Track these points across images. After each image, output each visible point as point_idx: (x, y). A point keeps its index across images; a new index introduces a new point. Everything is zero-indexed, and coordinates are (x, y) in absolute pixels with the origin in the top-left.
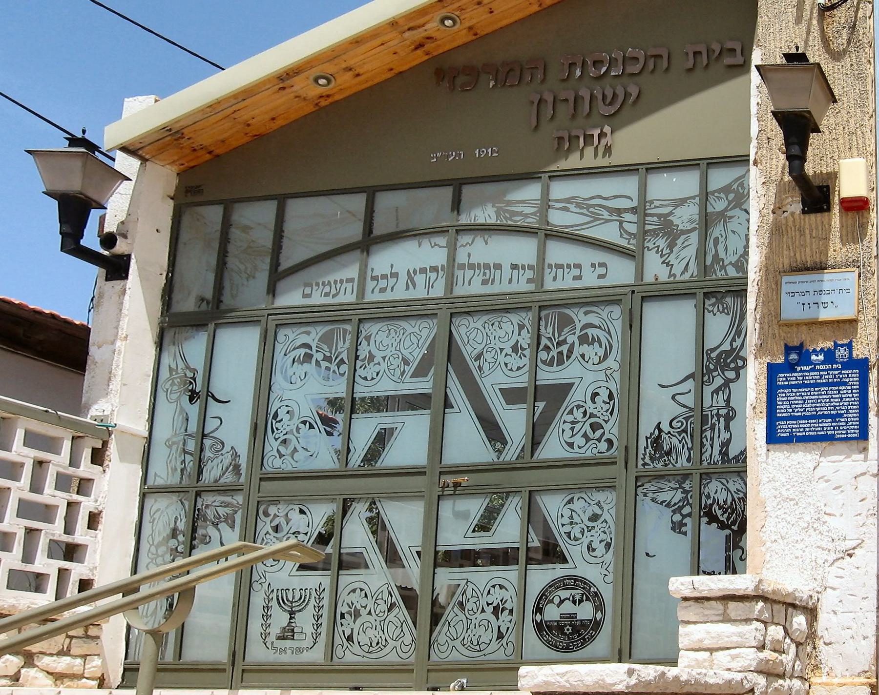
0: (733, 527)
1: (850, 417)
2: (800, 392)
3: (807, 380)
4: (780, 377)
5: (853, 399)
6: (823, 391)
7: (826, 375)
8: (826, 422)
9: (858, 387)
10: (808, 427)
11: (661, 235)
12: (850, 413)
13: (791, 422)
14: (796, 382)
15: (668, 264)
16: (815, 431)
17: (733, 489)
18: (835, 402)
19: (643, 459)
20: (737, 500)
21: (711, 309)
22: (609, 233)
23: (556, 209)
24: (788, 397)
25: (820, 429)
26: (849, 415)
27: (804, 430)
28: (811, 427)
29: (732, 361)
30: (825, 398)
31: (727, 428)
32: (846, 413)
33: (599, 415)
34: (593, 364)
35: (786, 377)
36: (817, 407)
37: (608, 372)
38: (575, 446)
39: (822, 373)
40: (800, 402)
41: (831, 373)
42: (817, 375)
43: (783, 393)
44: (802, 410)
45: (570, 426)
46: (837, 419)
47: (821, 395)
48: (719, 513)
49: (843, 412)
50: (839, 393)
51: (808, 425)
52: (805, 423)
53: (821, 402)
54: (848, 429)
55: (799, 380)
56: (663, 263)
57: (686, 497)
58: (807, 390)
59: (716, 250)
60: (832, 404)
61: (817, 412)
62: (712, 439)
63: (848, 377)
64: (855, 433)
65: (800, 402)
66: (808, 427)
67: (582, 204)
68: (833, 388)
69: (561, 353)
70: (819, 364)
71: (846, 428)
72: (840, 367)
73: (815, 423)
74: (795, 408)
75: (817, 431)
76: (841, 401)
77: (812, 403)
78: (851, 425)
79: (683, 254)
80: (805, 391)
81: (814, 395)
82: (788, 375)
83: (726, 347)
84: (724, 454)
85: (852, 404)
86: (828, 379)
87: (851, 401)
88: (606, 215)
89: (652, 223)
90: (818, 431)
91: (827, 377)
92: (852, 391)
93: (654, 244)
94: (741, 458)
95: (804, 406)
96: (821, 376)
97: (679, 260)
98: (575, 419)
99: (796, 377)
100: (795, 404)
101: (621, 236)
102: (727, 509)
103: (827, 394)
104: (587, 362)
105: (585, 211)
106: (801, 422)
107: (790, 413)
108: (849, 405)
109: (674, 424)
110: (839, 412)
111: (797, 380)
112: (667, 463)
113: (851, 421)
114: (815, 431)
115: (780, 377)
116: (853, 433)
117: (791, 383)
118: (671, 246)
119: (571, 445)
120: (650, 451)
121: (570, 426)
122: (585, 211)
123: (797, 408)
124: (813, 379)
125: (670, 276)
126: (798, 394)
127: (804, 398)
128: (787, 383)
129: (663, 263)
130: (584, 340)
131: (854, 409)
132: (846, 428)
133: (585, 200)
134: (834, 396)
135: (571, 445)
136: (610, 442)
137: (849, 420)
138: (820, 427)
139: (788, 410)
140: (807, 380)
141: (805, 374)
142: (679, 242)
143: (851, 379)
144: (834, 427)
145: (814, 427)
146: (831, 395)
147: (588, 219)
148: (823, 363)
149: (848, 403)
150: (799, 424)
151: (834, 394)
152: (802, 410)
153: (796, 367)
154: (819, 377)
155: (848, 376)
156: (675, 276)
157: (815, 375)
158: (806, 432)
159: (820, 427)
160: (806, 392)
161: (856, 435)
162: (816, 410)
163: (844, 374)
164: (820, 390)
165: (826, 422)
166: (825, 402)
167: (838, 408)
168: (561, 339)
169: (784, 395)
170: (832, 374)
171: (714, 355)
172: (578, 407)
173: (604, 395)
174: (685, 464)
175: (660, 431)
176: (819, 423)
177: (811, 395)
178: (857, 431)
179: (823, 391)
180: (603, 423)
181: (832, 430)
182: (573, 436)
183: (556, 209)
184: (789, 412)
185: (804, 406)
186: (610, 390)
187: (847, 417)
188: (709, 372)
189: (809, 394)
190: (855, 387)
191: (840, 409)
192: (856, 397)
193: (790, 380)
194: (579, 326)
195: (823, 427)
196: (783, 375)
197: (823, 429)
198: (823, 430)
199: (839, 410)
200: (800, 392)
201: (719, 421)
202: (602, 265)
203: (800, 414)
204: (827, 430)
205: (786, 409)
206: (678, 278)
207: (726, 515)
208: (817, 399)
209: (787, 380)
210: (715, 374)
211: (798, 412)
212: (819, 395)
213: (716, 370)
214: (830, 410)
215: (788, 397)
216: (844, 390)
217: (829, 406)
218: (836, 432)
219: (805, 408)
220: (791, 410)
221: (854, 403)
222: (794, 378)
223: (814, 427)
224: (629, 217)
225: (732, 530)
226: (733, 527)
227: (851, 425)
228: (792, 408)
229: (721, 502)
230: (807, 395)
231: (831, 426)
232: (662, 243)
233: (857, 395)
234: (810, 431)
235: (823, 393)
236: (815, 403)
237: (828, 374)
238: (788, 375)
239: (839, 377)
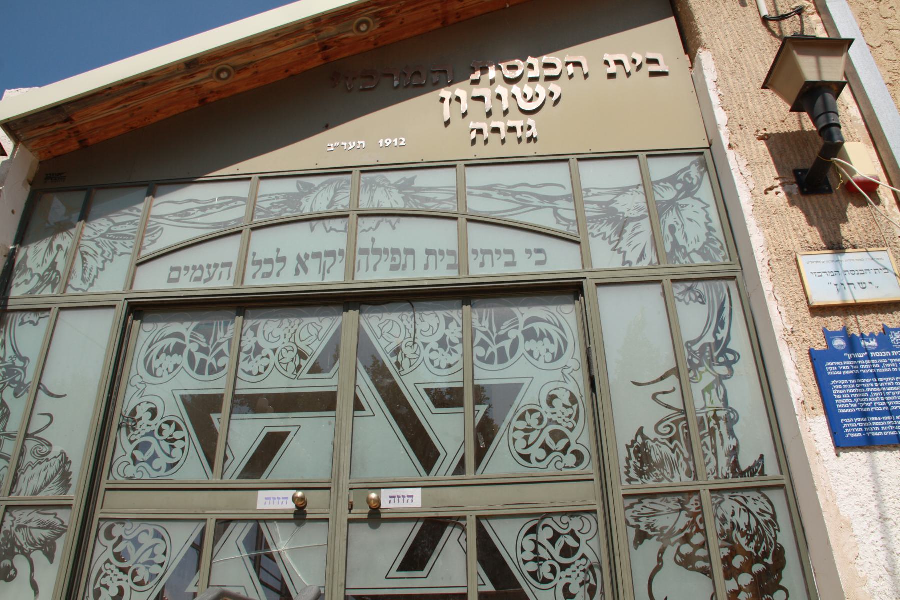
0: (765, 560)
6: (889, 382)
11: (605, 221)
15: (620, 252)
17: (755, 509)
19: (627, 473)
20: (763, 523)
21: (681, 297)
22: (544, 219)
23: (476, 195)
29: (720, 355)
31: (731, 433)
33: (560, 421)
34: (546, 362)
37: (566, 372)
38: (533, 459)
39: (881, 361)
45: (523, 434)
47: (888, 386)
48: (743, 541)
51: (883, 423)
52: (879, 421)
56: (614, 250)
57: (694, 522)
58: (869, 381)
59: (675, 238)
62: (714, 447)
67: (508, 192)
69: (502, 351)
70: (874, 351)
79: (636, 240)
80: (866, 383)
83: (709, 339)
84: (735, 465)
88: (536, 202)
89: (591, 211)
91: (889, 365)
93: (599, 230)
94: (757, 471)
95: (871, 399)
96: (881, 365)
97: (632, 247)
98: (528, 426)
101: (558, 223)
102: (752, 537)
104: (538, 360)
105: (511, 198)
107: (855, 408)
109: (661, 428)
112: (661, 477)
118: (621, 233)
119: (527, 458)
120: (635, 462)
121: (523, 434)
122: (511, 198)
125: (624, 263)
129: (614, 250)
130: (530, 335)
133: (510, 187)
135: (527, 458)
136: (578, 455)
139: (852, 405)
142: (629, 228)
147: (518, 206)
148: (878, 350)
156: (630, 263)
160: (868, 383)
164: (885, 381)
168: (502, 333)
171: (696, 348)
172: (532, 412)
173: (565, 398)
174: (686, 479)
175: (645, 438)
179: (889, 382)
180: (567, 432)
182: (528, 447)
183: (476, 195)
184: (853, 408)
185: (871, 399)
186: (570, 392)
188: (693, 367)
194: (522, 321)
201: (718, 424)
202: (539, 251)
205: (848, 403)
206: (634, 265)
207: (753, 545)
210: (701, 369)
213: (701, 365)
219: (873, 402)
220: (855, 406)
224: (561, 204)
225: (766, 564)
226: (765, 560)
228: (855, 403)
229: (742, 527)
230: (870, 387)
232: (608, 230)
235: (890, 384)
237: (889, 362)
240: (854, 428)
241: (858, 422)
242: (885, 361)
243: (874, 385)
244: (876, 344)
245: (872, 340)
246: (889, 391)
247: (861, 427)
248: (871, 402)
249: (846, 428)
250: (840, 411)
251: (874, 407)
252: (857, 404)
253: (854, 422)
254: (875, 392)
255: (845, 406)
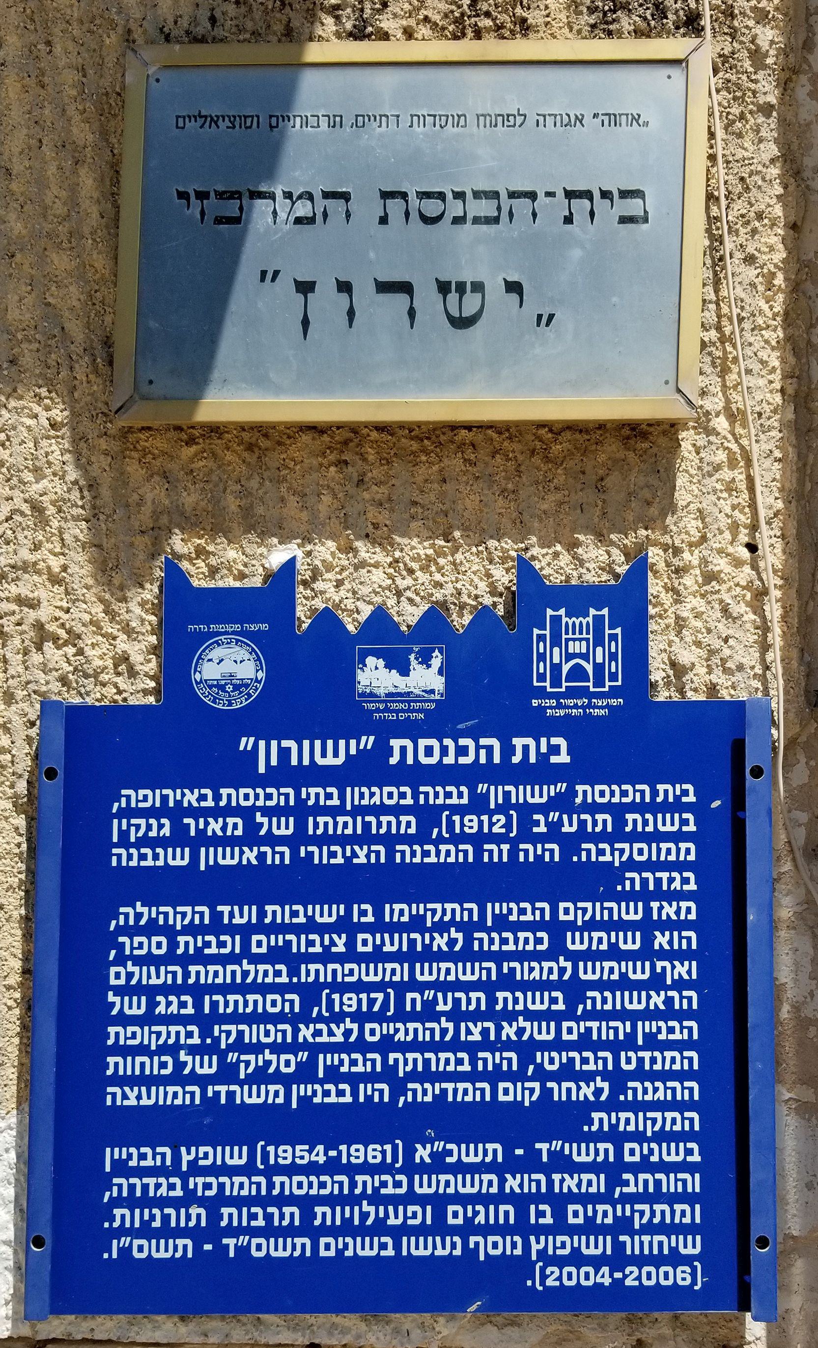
1: (639, 1137)
2: (276, 928)
3: (324, 840)
4: (129, 813)
5: (658, 1000)
6: (441, 927)
7: (461, 810)
8: (460, 1168)
9: (689, 910)
10: (331, 1201)
12: (637, 1106)
13: (208, 1156)
14: (250, 855)
16: (380, 1228)
18: (529, 1015)
24: (185, 961)
25: (417, 1215)
26: (626, 1120)
27: (308, 1215)
28: (353, 1200)
30: (458, 986)
32: (612, 1105)
35: (177, 813)
36: (404, 1047)
40: (273, 1003)
41: (495, 795)
42: (397, 811)
43: (151, 929)
44: (287, 1063)
46: (543, 1147)
47: (430, 956)
49: (587, 1091)
50: (557, 950)
51: (331, 1184)
52: (312, 1169)
53: (429, 1013)
54: (623, 1225)
55: (272, 840)
58: (327, 915)
60: (509, 1031)
61: (398, 1089)
63: (618, 835)
64: (675, 1259)
65: (273, 1003)
66: (331, 1201)
68: (513, 910)
70: (413, 731)
71: (605, 1214)
72: (563, 758)
73: (383, 1168)
74: (240, 1046)
75: (397, 1233)
76: (569, 1014)
77: (359, 1017)
78: (644, 1197)
80: (311, 926)
81: (378, 956)
82: (191, 798)
85: (652, 1042)
86: (479, 840)
87: (649, 1015)
90: (404, 1230)
91: (471, 824)
92: (647, 940)
95: (306, 1033)
99: (247, 814)
100: (235, 1018)
103: (468, 955)
106: (285, 1154)
107: (203, 1081)
108: (630, 1043)
110: (560, 1091)
111: (251, 837)
113: (645, 1165)
114: (380, 1228)
115: (129, 813)
116: (658, 1261)
117: (207, 857)
123: (257, 1048)
124: (366, 838)
126: (260, 944)
127: (310, 972)
128: (180, 859)
131: (665, 1076)
132: (605, 1214)
134: (522, 971)
137: (632, 1153)
138: (423, 1200)
140: (324, 840)
141: (313, 793)
143: (640, 852)
144: (521, 1201)
145: (376, 1199)
146: (499, 957)
149: (623, 1028)
150: (270, 1171)
151: (521, 956)
152: (287, 1063)
153: (246, 743)
154: (409, 824)
155: (620, 822)
157: (380, 810)
158: (315, 1234)
159: (423, 1200)
160: (323, 929)
161: (682, 1276)
162: (389, 1074)
163: (594, 808)
164: (417, 923)
165: (460, 1168)
166: (456, 1015)
167: (550, 1062)
169: (158, 945)
170: (504, 808)
176: (411, 1168)
177: (351, 955)
178: (692, 1247)
179: (441, 927)
181: (503, 1230)
185: (306, 1033)
187: (617, 1137)
189: (340, 947)
190: (669, 910)
191: (567, 1072)
192: (680, 985)
193: (203, 839)
195: (439, 1202)
196: (149, 797)
197: (440, 1215)
198: (440, 1228)
199: (558, 1076)
200: (276, 928)
203: (274, 1094)
204: (468, 1228)
205: (173, 1050)
208: (401, 988)
209: (179, 838)
211: (261, 1076)
212: (410, 957)
214: (495, 1076)
215: (185, 961)
216: (591, 925)
217: (486, 1044)
218: (535, 1247)
219: (315, 1049)
220: (208, 1067)
221: (662, 1029)
222: (236, 825)
223: (376, 1199)
227: (644, 1197)
230: (326, 957)
231: (501, 1198)
233: (681, 970)
234: (347, 1229)
235: (440, 942)
236: (381, 1017)
237: (479, 805)
238: (191, 798)
239: (554, 828)
240: (162, 1202)
241: (195, 1169)
242: (459, 796)
243: (351, 944)
244: (438, 683)
245: (425, 659)
246: (421, 987)
247: (202, 1202)
248: (306, 1046)
249: (118, 1202)
250: (114, 1095)
251: (313, 1079)
252: (223, 1055)
253: (175, 1170)
254: (343, 988)
255: (151, 1066)
